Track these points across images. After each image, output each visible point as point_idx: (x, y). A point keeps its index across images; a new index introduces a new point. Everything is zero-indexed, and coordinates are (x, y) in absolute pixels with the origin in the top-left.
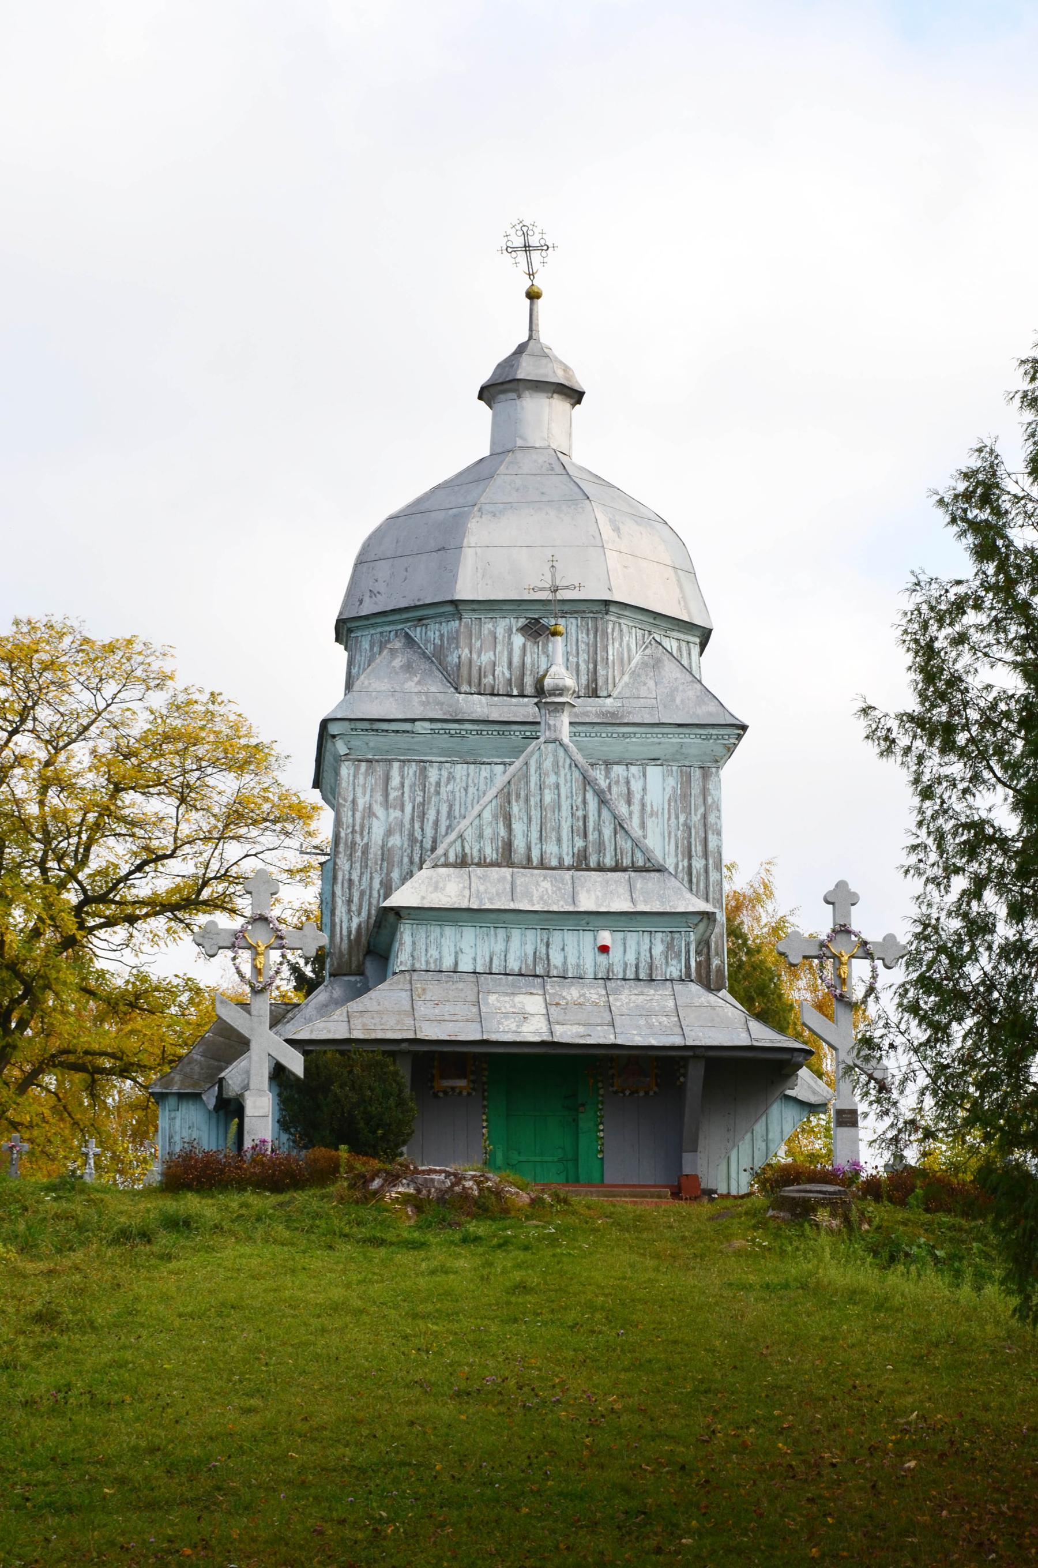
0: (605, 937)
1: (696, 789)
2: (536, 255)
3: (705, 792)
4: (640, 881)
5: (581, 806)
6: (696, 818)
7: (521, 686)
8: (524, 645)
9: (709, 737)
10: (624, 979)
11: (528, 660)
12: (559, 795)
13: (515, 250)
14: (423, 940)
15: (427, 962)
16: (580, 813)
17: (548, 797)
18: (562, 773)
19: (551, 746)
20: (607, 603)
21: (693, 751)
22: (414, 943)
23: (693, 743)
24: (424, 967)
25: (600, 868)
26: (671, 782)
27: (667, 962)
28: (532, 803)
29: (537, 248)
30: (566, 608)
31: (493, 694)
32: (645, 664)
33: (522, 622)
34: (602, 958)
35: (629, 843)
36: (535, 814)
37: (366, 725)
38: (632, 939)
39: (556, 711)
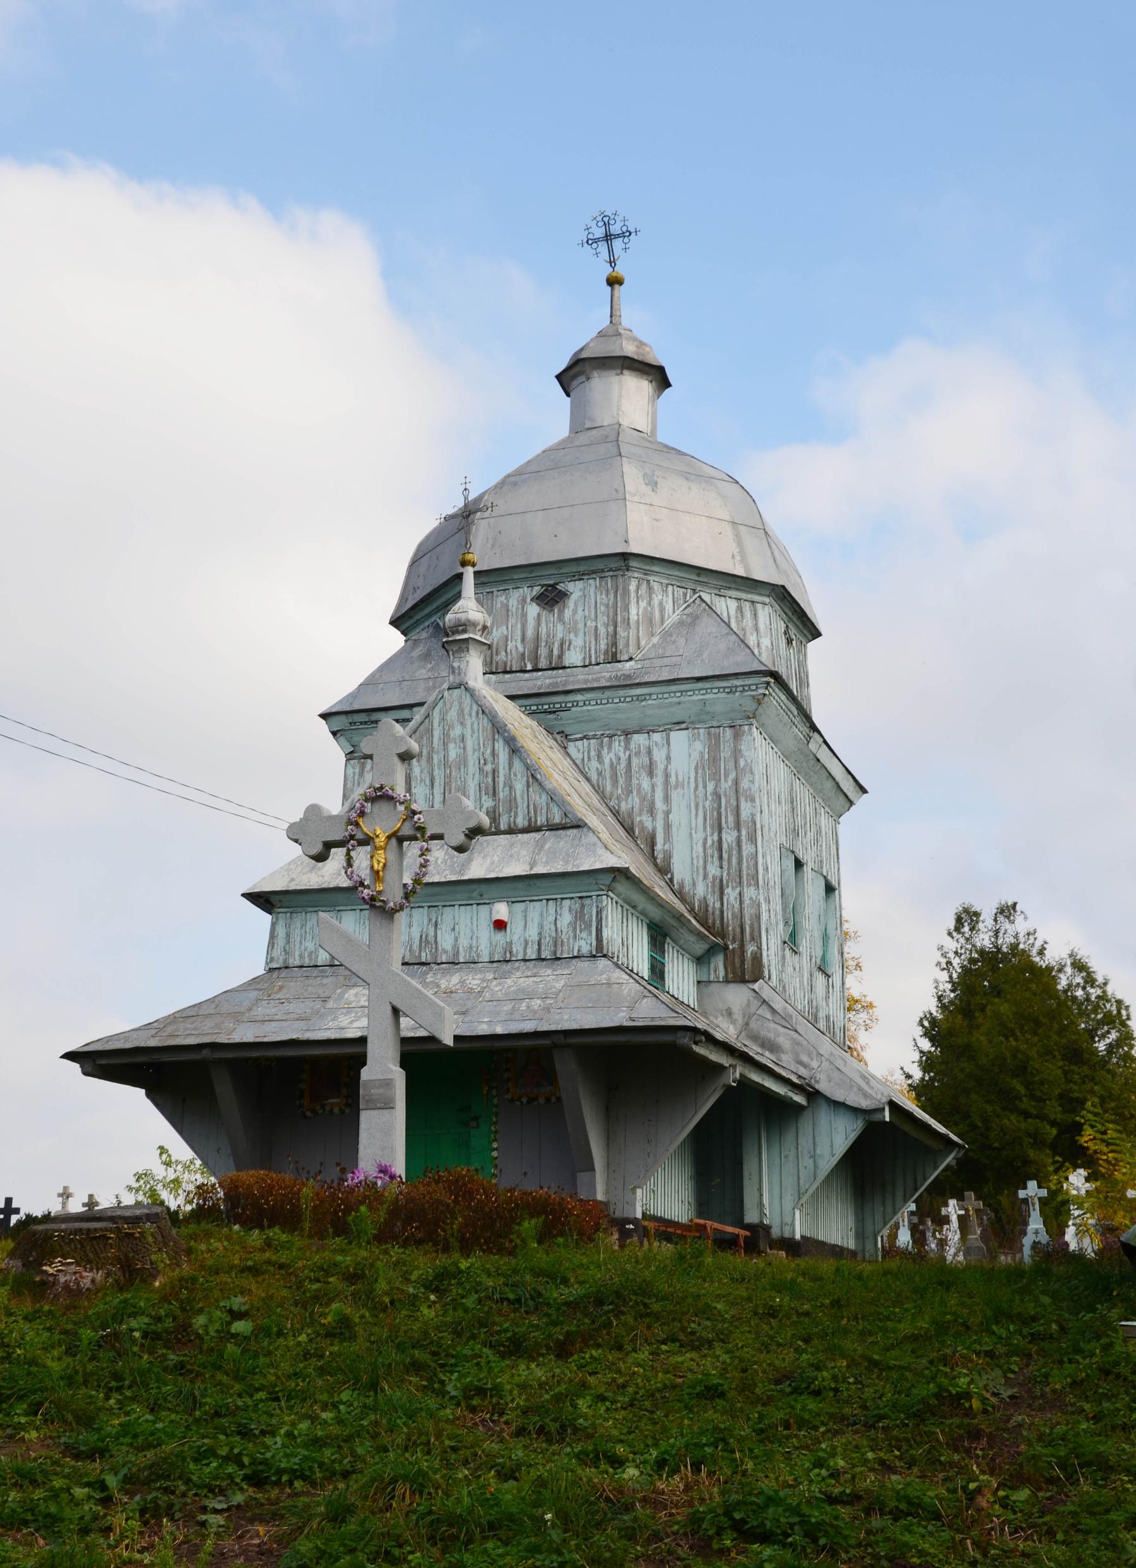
0: (501, 911)
1: (726, 752)
2: (617, 244)
3: (736, 754)
4: (551, 840)
5: (490, 759)
6: (726, 785)
7: (536, 658)
8: (539, 614)
9: (732, 691)
10: (525, 960)
11: (543, 630)
12: (464, 748)
13: (596, 241)
14: (298, 931)
15: (301, 956)
16: (489, 768)
17: (453, 754)
18: (468, 723)
19: (456, 692)
20: (625, 556)
21: (718, 708)
22: (288, 935)
23: (716, 698)
24: (297, 963)
25: (511, 831)
26: (698, 746)
27: (575, 936)
28: (435, 761)
29: (618, 236)
30: (582, 568)
31: (505, 672)
32: (681, 623)
33: (537, 590)
34: (500, 937)
35: (544, 797)
36: (439, 774)
37: (362, 717)
38: (535, 910)
39: (460, 650)
